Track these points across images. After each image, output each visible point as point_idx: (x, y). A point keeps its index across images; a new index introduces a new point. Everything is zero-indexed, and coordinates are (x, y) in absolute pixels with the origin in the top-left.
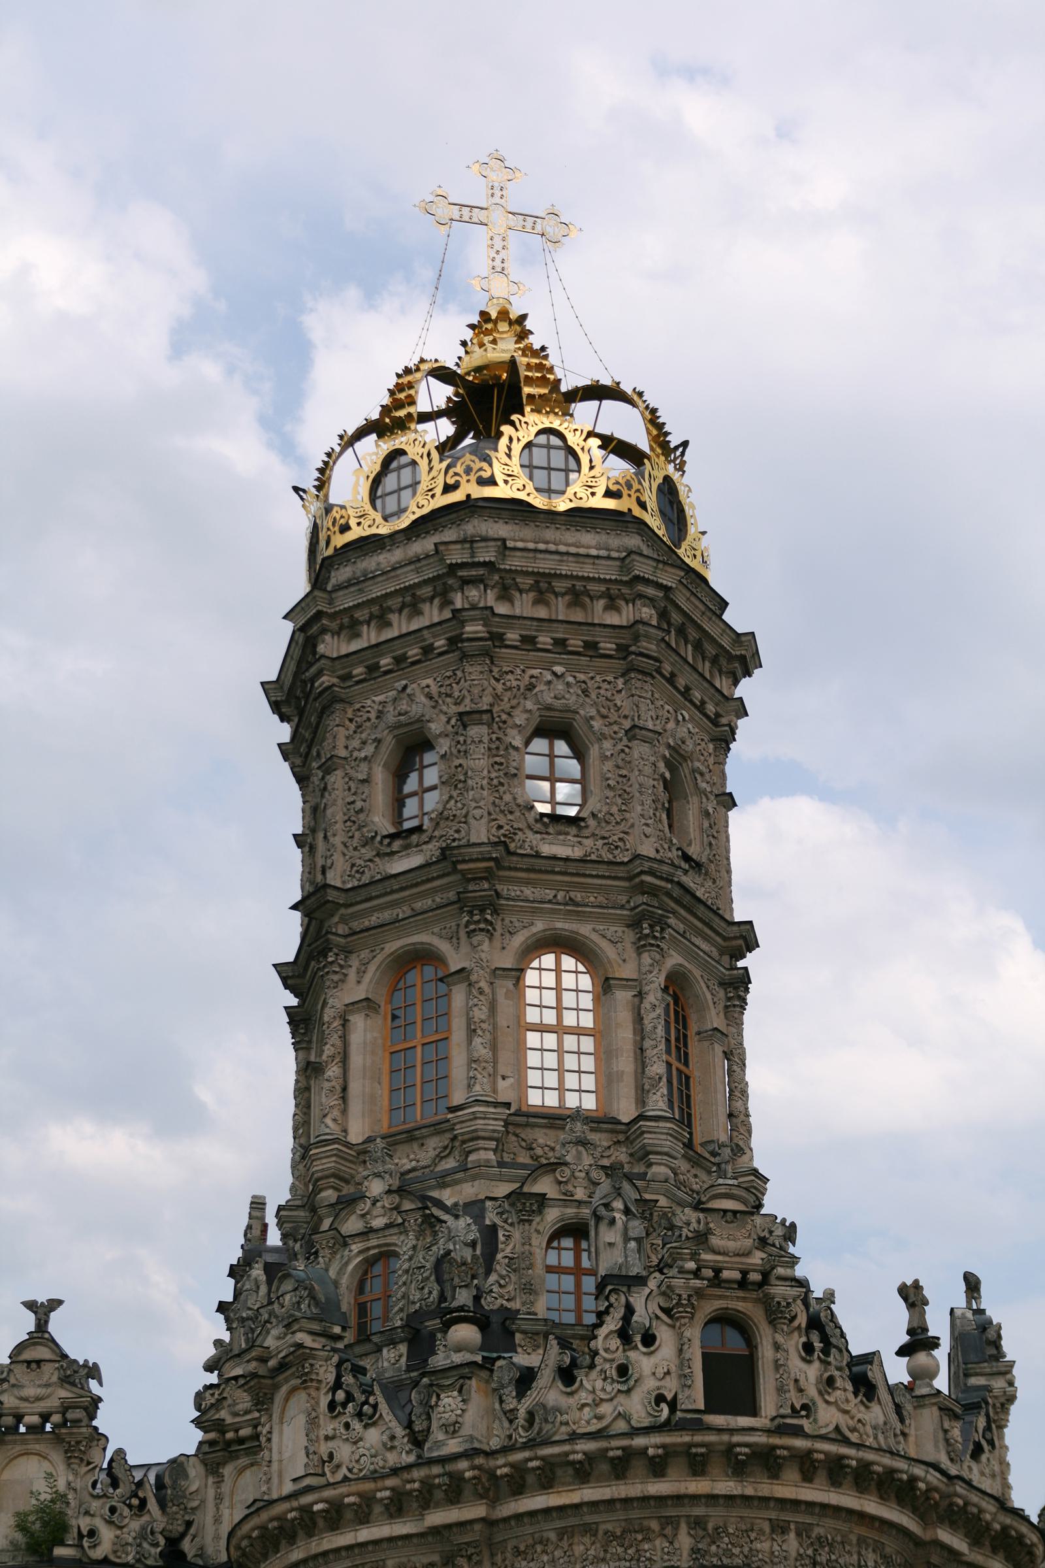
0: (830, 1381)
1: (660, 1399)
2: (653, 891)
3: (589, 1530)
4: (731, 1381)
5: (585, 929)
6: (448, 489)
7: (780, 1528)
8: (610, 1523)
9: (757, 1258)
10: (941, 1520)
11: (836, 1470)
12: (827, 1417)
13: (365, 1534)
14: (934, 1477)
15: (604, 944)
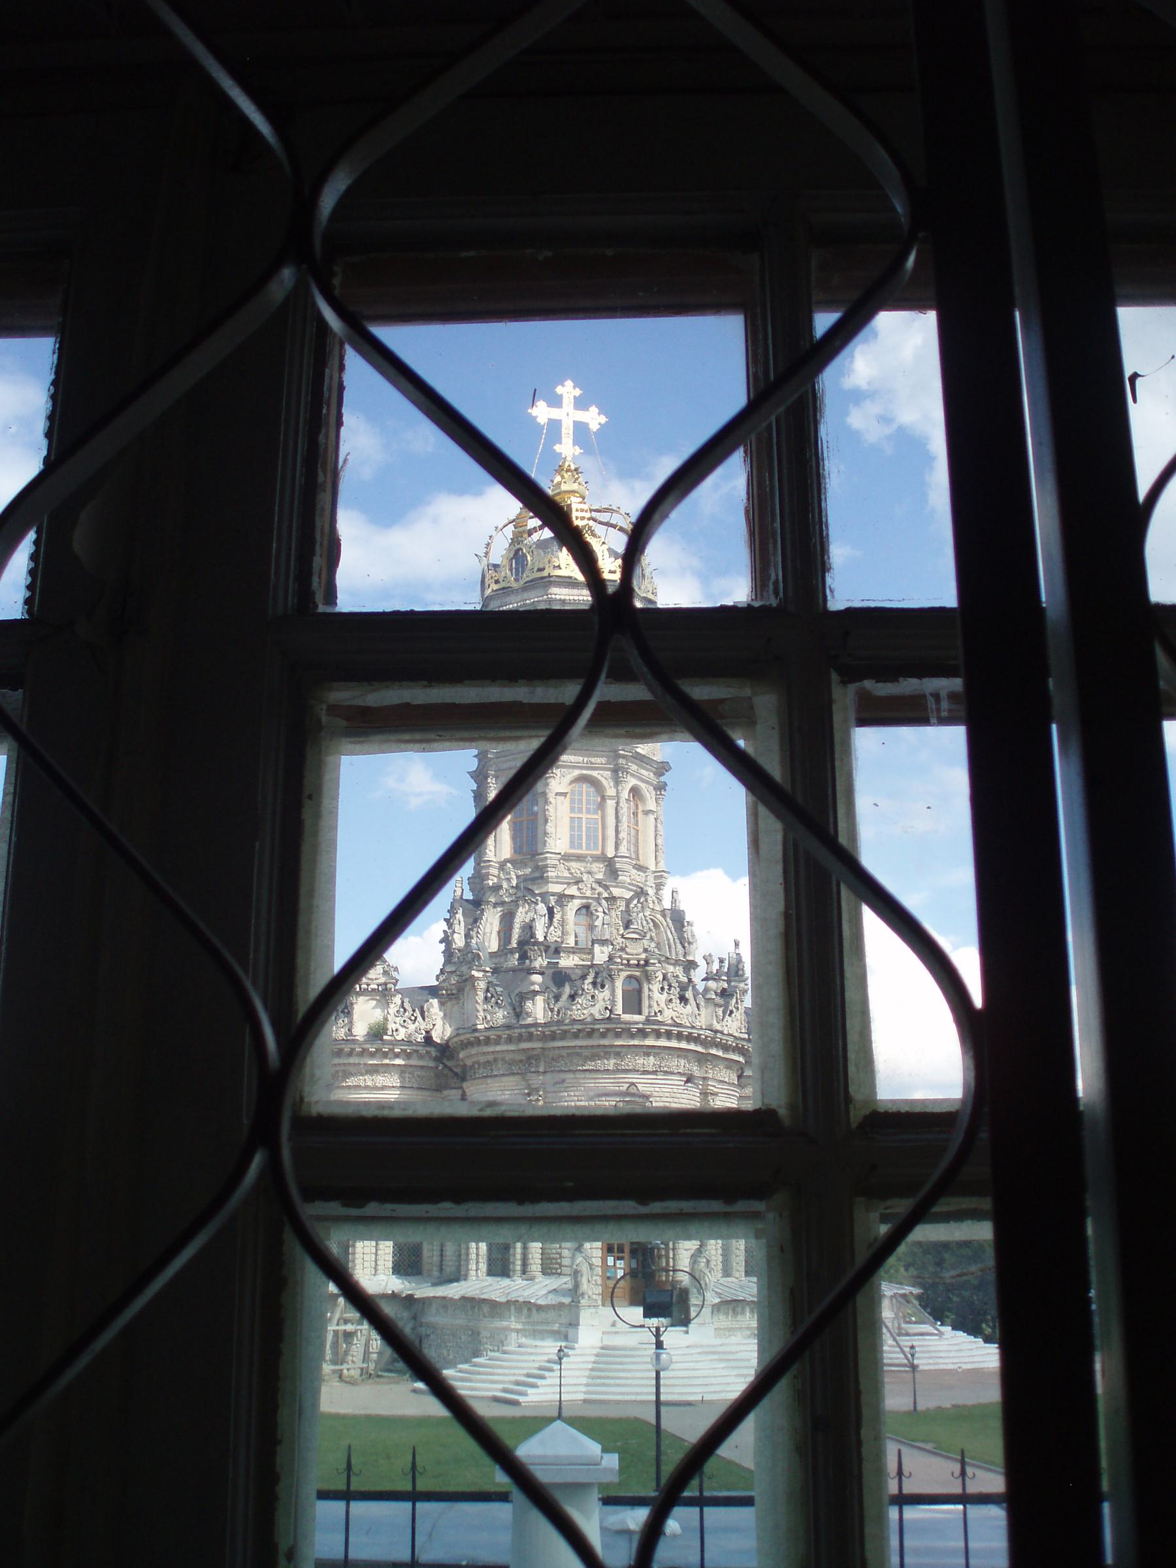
0: (671, 1000)
1: (606, 1008)
2: (624, 757)
3: (578, 1054)
4: (634, 1001)
5: (594, 773)
6: (541, 570)
7: (648, 1055)
8: (586, 1053)
9: (643, 956)
10: (711, 1046)
11: (669, 1035)
12: (668, 1015)
13: (498, 1048)
14: (708, 1033)
15: (603, 780)
